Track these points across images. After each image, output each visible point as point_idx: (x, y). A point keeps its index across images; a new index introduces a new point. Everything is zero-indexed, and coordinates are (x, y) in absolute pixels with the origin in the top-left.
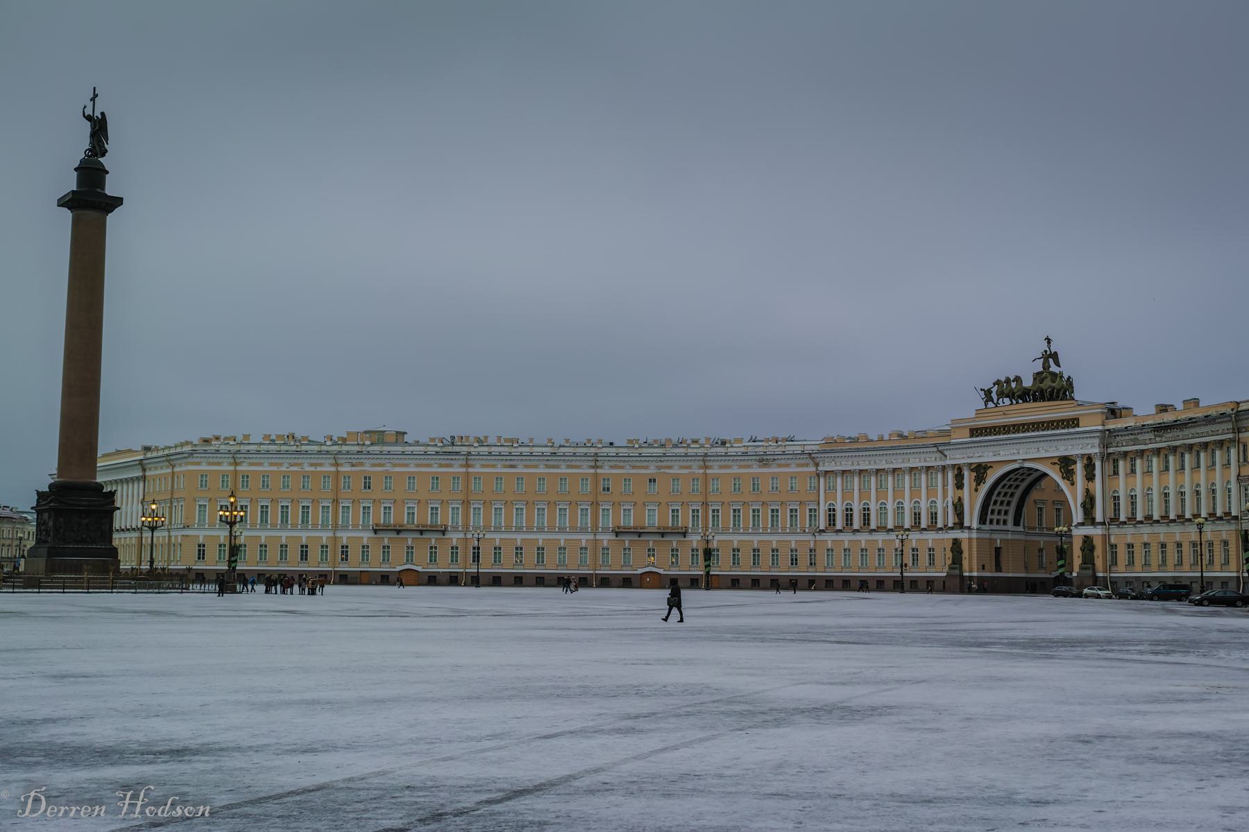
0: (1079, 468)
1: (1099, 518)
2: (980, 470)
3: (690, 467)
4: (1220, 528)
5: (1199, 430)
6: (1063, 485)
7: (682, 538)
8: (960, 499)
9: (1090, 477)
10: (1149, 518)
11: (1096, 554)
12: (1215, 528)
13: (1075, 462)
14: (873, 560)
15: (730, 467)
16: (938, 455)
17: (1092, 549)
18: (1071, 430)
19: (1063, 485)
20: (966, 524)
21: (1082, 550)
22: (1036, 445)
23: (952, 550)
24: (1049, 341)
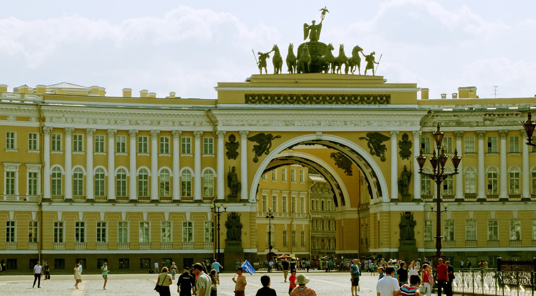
0: (393, 147)
1: (417, 196)
2: (262, 142)
11: (416, 229)
13: (388, 139)
17: (413, 224)
18: (383, 106)
20: (244, 195)
21: (401, 226)
23: (228, 225)
24: (324, 11)
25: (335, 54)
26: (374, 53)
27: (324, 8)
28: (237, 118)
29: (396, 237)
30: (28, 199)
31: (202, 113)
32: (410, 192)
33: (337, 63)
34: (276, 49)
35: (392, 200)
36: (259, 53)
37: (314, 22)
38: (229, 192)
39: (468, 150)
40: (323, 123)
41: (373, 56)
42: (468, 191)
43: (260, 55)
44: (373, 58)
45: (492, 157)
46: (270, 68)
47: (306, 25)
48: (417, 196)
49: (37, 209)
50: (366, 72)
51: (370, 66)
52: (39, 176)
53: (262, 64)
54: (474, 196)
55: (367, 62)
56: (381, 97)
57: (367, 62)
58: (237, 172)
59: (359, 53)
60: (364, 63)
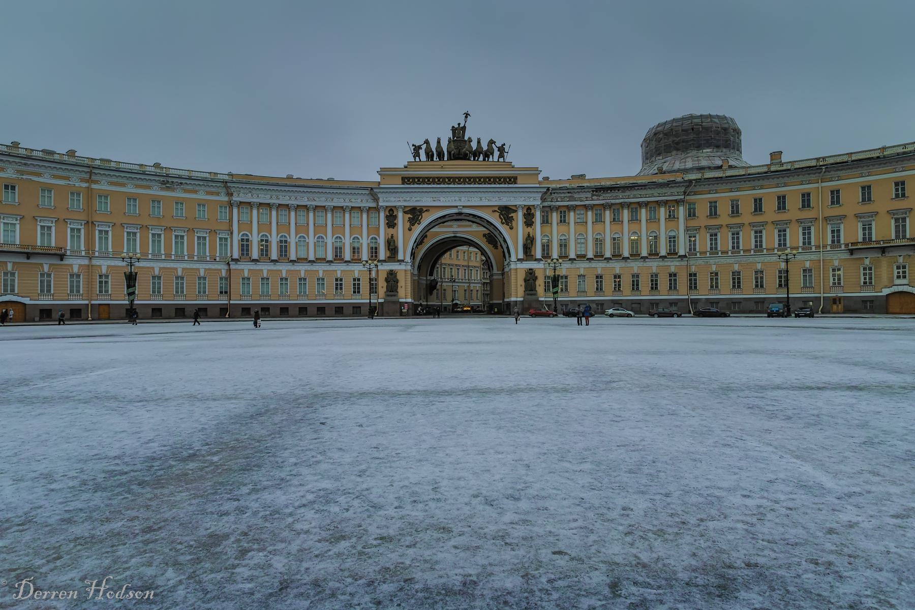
0: (520, 217)
2: (415, 214)
3: (67, 178)
4: (666, 264)
5: (643, 192)
6: (503, 229)
7: (56, 261)
8: (392, 236)
9: (529, 222)
10: (581, 257)
11: (537, 283)
12: (661, 264)
13: (516, 211)
14: (312, 287)
15: (123, 185)
16: (369, 198)
19: (503, 229)
20: (400, 257)
21: (525, 280)
22: (480, 195)
23: (387, 280)
24: (467, 115)
25: (474, 145)
28: (394, 195)
29: (521, 290)
30: (218, 259)
31: (367, 192)
32: (533, 253)
33: (476, 154)
34: (427, 142)
35: (519, 260)
37: (459, 124)
38: (388, 255)
39: (579, 221)
40: (463, 199)
42: (579, 253)
45: (599, 226)
46: (423, 157)
48: (539, 255)
49: (226, 267)
51: (501, 156)
52: (229, 240)
53: (416, 153)
54: (584, 256)
56: (510, 178)
58: (395, 238)
60: (497, 153)
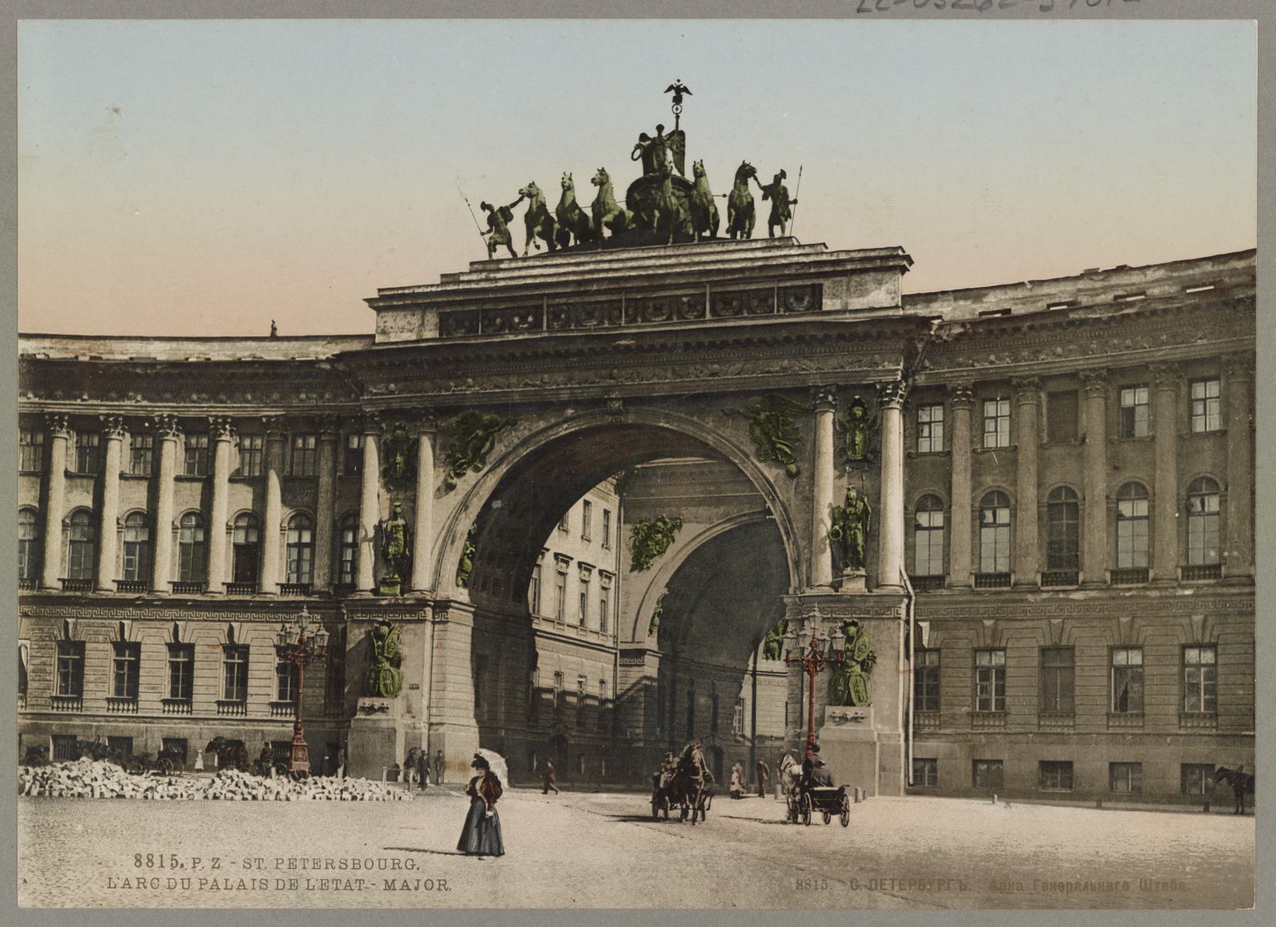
24: (679, 92)
26: (783, 174)
27: (674, 83)
34: (530, 192)
36: (484, 206)
37: (660, 128)
41: (784, 182)
43: (488, 213)
44: (785, 189)
47: (643, 137)
50: (771, 233)
51: (780, 215)
55: (769, 203)
57: (770, 202)
59: (751, 181)
60: (763, 209)
